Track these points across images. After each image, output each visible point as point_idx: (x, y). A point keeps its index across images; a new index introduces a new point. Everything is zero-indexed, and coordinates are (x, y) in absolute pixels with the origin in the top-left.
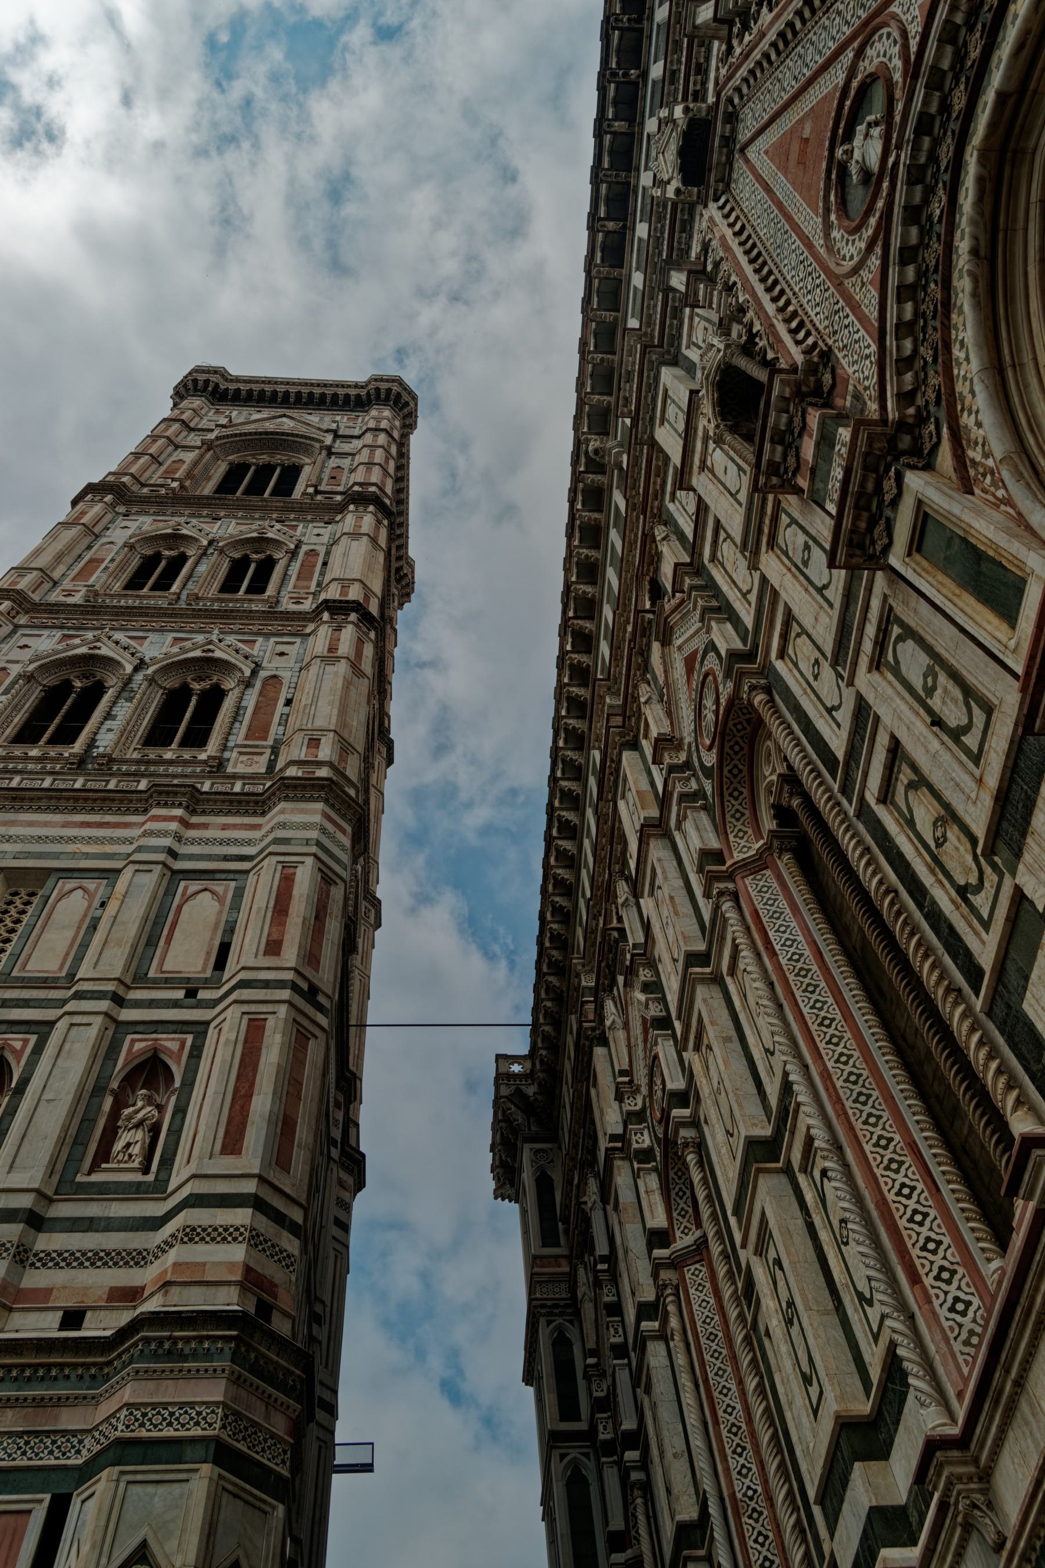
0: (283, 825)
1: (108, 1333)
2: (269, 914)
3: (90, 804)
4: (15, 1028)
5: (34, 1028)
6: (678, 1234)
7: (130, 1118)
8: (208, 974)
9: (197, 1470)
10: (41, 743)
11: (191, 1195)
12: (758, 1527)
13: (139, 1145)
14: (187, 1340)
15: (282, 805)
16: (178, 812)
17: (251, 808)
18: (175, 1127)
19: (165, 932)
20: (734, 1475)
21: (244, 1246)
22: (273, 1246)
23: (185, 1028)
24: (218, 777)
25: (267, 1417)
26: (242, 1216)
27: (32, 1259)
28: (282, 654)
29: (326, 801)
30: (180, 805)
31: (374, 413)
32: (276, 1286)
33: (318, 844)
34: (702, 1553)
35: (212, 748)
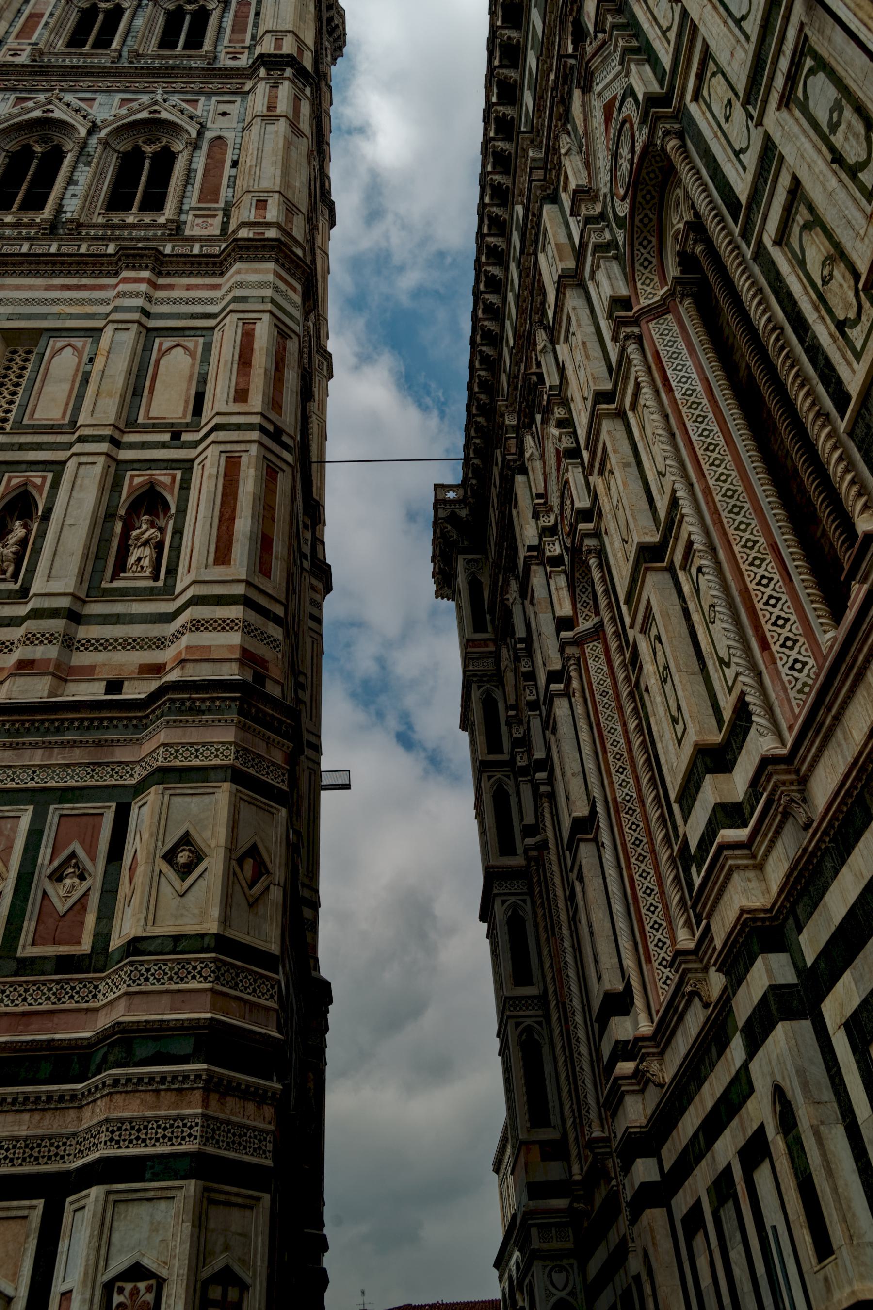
0: (240, 285)
1: (142, 696)
2: (235, 366)
3: (66, 267)
4: (34, 467)
5: (49, 467)
6: (581, 620)
7: (138, 538)
8: (188, 419)
9: (220, 787)
10: (13, 209)
11: (193, 596)
12: (632, 819)
13: (148, 559)
14: (203, 700)
15: (238, 265)
16: (146, 274)
17: (210, 268)
18: (175, 545)
19: (148, 384)
20: (617, 786)
21: (239, 633)
23: (174, 465)
24: (178, 240)
25: (268, 752)
26: (235, 612)
27: (76, 645)
28: (224, 114)
29: (277, 261)
30: (147, 267)
32: (267, 662)
33: (273, 301)
34: (591, 836)
35: (169, 211)
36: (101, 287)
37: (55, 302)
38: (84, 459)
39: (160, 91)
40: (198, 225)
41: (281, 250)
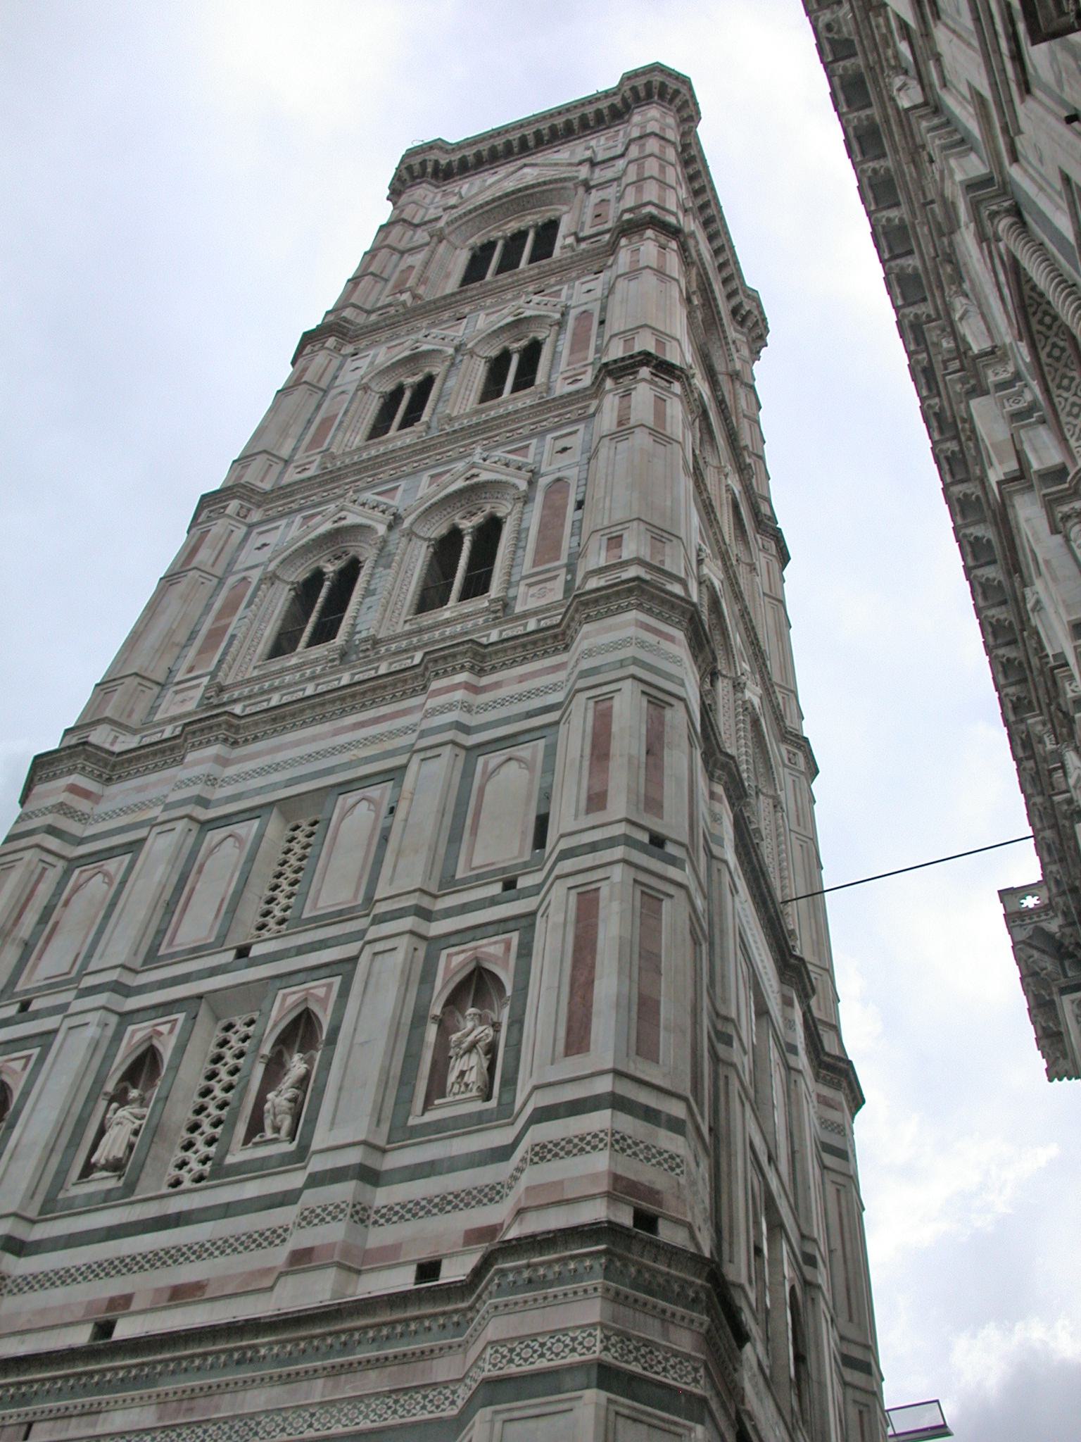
0: (589, 653)
2: (586, 764)
3: (359, 700)
7: (459, 1045)
8: (527, 858)
9: (580, 1397)
10: (299, 649)
11: (535, 1110)
14: (549, 1264)
15: (586, 628)
16: (463, 677)
17: (550, 645)
19: (469, 822)
21: (607, 1152)
22: (647, 1148)
24: (507, 622)
25: (665, 1335)
26: (600, 1120)
27: (374, 1217)
28: (565, 450)
29: (639, 607)
30: (463, 667)
31: (636, 118)
32: (658, 1192)
35: (495, 590)
36: (404, 712)
37: (344, 748)
38: (379, 946)
39: (479, 450)
40: (533, 596)
41: (643, 591)
